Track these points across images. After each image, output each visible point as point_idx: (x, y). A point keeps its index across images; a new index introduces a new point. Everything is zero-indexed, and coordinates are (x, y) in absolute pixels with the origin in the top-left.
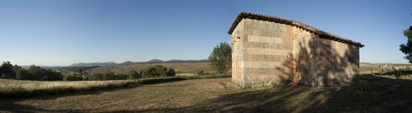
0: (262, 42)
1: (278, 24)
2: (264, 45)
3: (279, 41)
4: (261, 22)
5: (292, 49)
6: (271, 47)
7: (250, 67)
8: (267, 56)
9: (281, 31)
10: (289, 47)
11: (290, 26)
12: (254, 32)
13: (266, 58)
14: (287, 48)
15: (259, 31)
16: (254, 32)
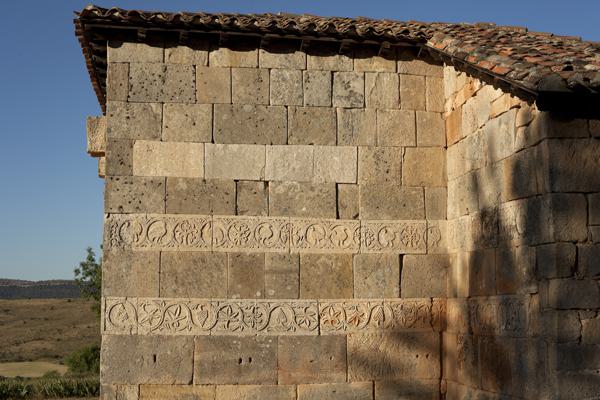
0: (227, 176)
1: (331, 61)
2: (236, 197)
3: (340, 164)
4: (221, 57)
5: (433, 208)
6: (286, 208)
7: (143, 331)
8: (256, 261)
9: (357, 103)
10: (406, 195)
11: (418, 65)
12: (174, 117)
13: (248, 273)
14: (400, 208)
15: (203, 111)
16: (174, 117)
